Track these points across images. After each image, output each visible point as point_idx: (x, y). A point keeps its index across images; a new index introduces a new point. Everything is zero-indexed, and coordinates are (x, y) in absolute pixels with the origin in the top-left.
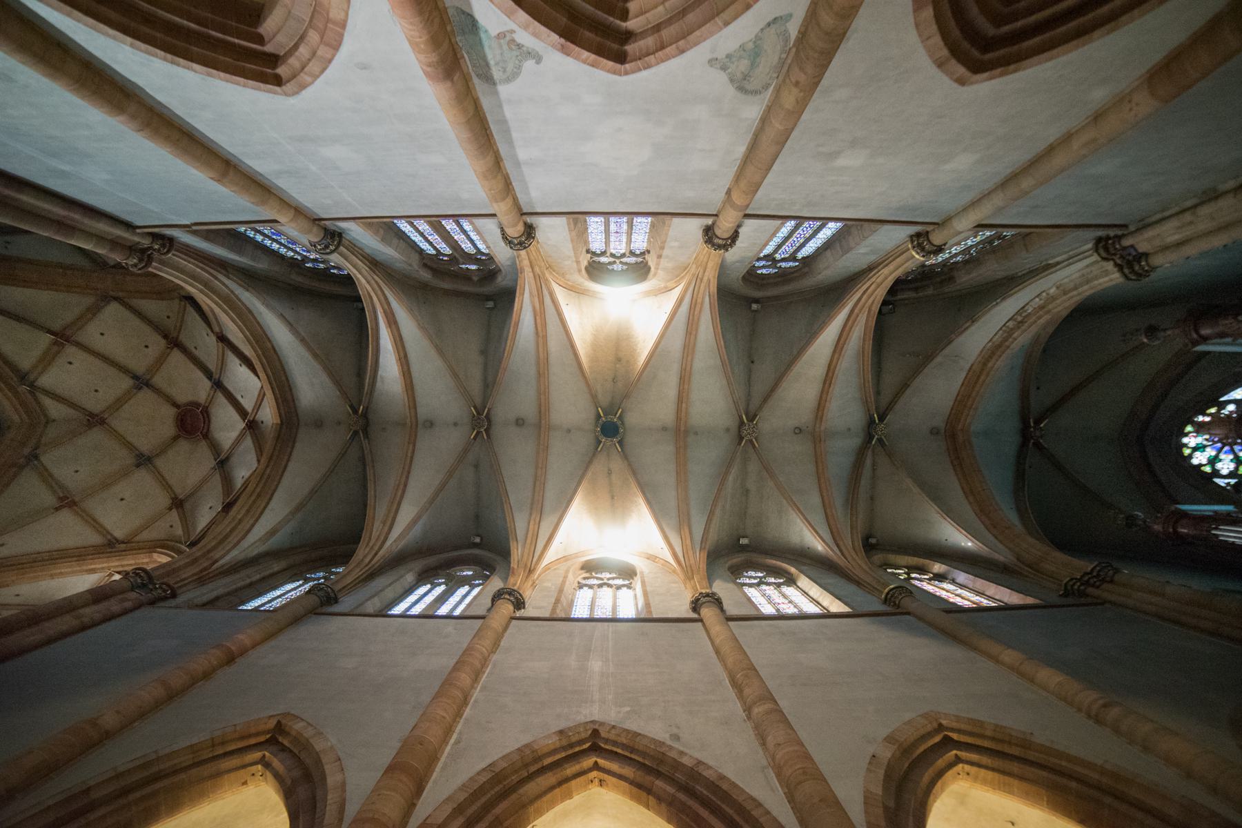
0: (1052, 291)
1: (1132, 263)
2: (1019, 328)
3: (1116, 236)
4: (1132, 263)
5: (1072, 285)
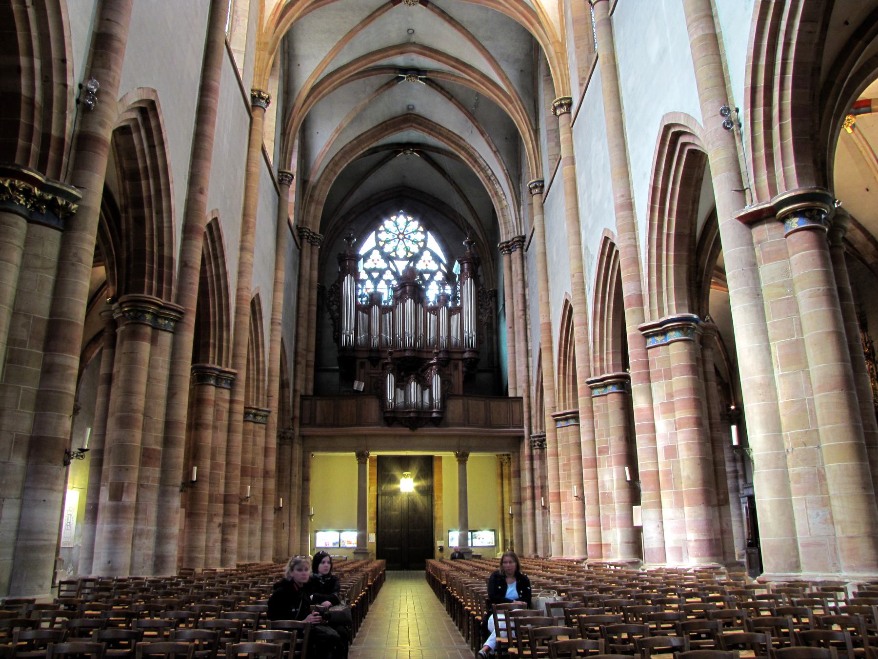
0: (505, 203)
1: (509, 247)
2: (486, 177)
3: (523, 245)
4: (509, 247)
5: (506, 213)
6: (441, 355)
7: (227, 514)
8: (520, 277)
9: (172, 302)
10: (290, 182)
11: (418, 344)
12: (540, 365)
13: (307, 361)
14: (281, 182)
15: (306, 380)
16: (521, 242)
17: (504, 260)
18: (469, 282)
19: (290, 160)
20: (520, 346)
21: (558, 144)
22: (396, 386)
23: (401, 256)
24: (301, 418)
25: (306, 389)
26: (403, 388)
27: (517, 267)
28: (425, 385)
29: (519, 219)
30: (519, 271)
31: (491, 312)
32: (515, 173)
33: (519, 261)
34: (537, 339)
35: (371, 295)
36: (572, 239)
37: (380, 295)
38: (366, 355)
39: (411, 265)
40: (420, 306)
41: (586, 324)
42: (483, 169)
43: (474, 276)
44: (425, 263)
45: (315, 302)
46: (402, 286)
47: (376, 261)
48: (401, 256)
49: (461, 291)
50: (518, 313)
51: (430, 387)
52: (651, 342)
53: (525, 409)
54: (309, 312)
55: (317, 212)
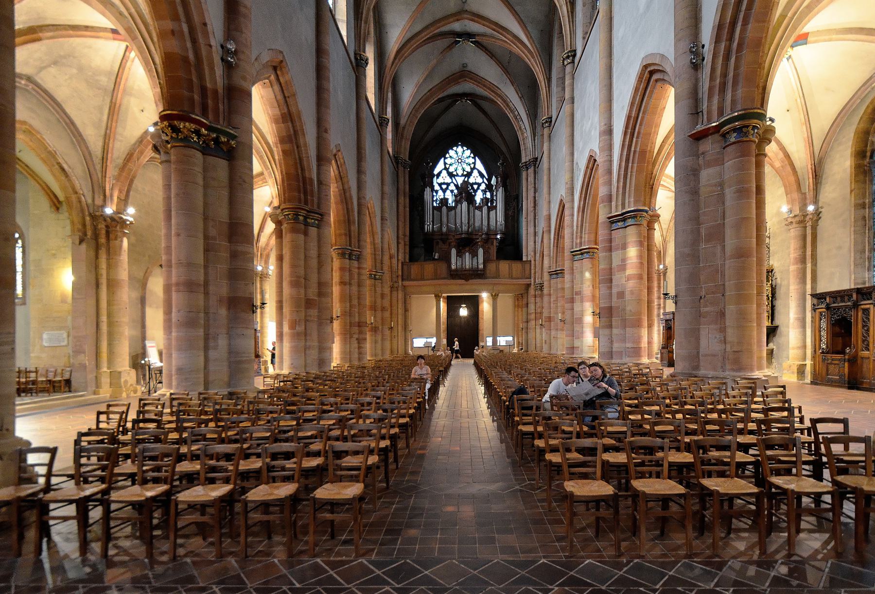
1: (527, 166)
6: (484, 236)
7: (360, 333)
8: (533, 185)
9: (315, 207)
10: (387, 124)
11: (470, 230)
12: (542, 241)
13: (405, 242)
14: (381, 124)
15: (405, 253)
16: (535, 162)
17: (524, 174)
18: (501, 190)
19: (386, 108)
20: (531, 230)
21: (564, 89)
22: (457, 256)
23: (460, 174)
24: (402, 276)
25: (405, 259)
26: (461, 257)
27: (531, 179)
28: (474, 254)
29: (534, 146)
30: (533, 182)
31: (514, 209)
32: (533, 114)
33: (532, 175)
34: (542, 225)
35: (441, 199)
36: (568, 158)
37: (447, 200)
38: (440, 237)
39: (466, 179)
40: (471, 206)
41: (573, 215)
42: (512, 111)
43: (505, 186)
44: (475, 178)
45: (408, 205)
46: (460, 193)
47: (445, 178)
48: (460, 174)
49: (496, 195)
50: (531, 209)
51: (477, 256)
52: (614, 226)
53: (532, 268)
54: (405, 213)
55: (406, 145)
